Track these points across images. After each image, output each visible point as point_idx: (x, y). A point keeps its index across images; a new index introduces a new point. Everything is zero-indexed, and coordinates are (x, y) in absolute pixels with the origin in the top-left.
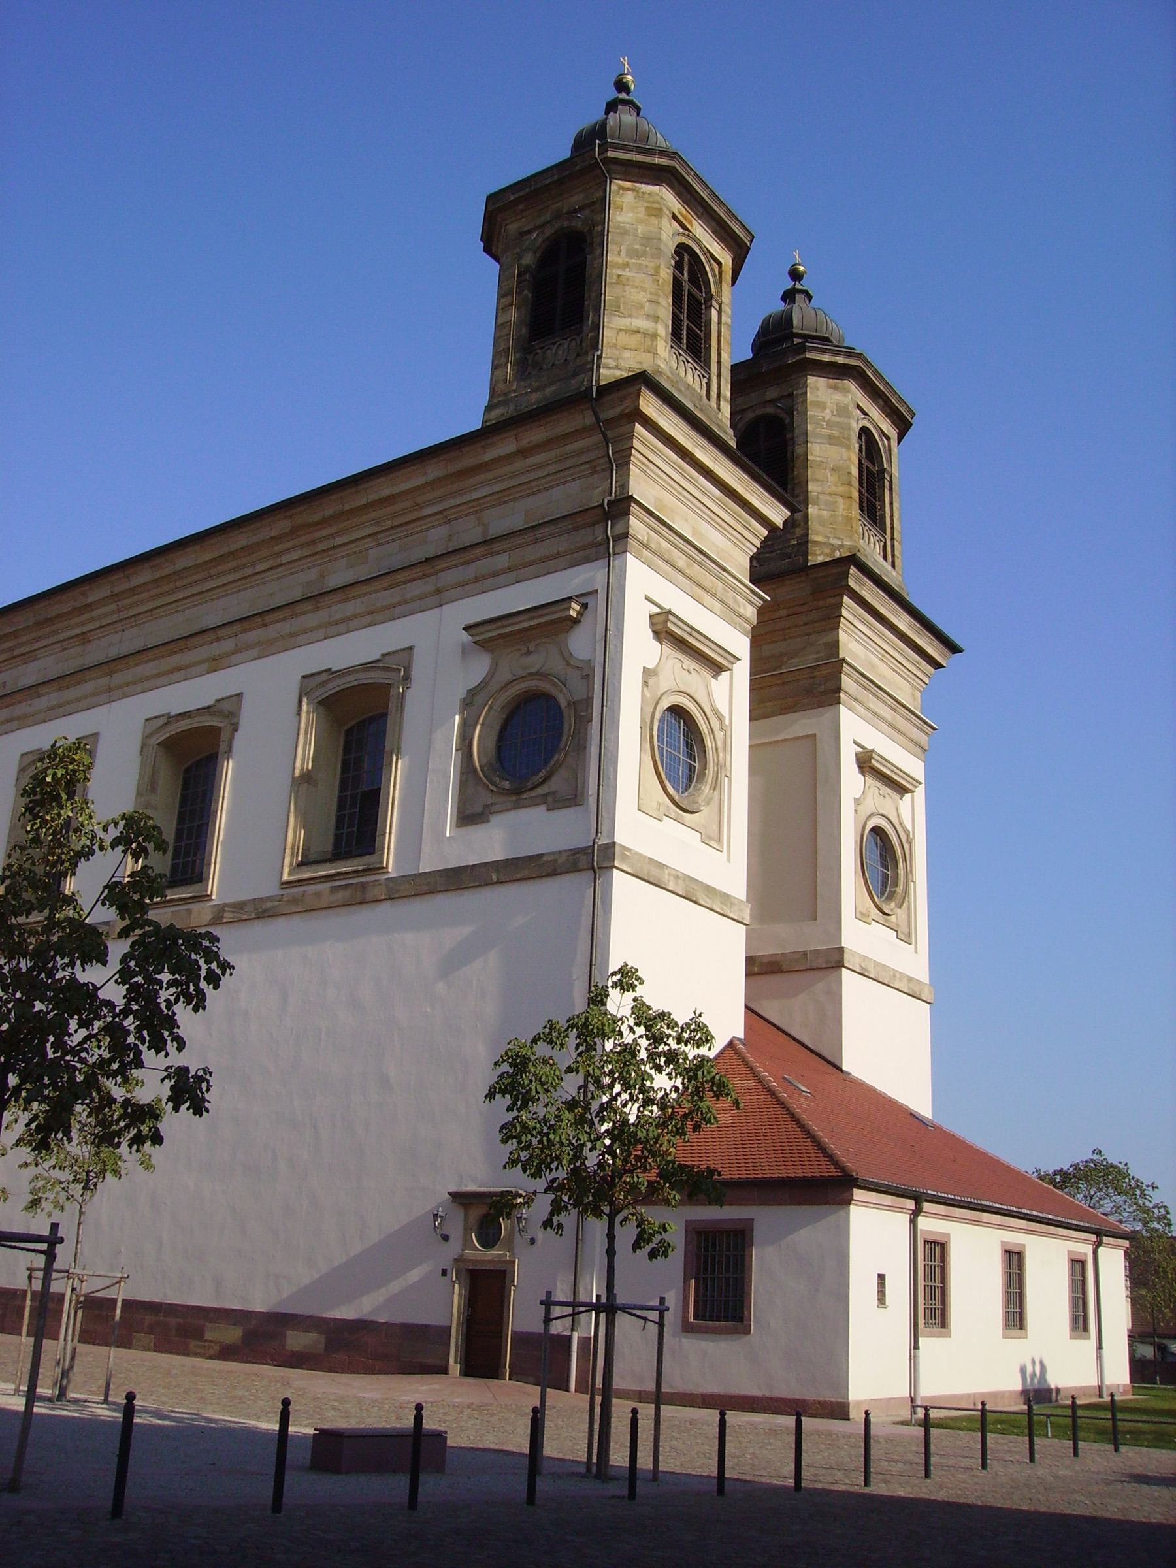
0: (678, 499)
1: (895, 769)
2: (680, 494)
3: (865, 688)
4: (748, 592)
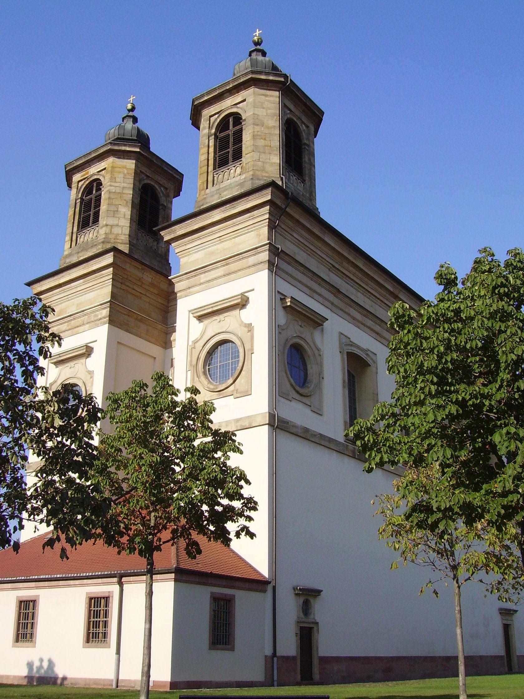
0: (69, 300)
1: (213, 305)
2: (68, 298)
3: (195, 276)
4: (100, 306)
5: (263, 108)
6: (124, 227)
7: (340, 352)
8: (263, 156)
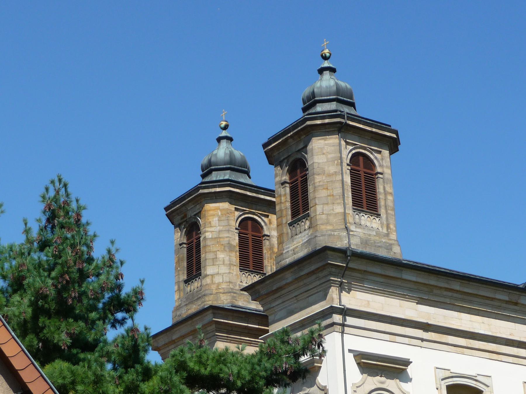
5: (324, 154)
6: (225, 275)
7: (437, 389)
8: (326, 207)
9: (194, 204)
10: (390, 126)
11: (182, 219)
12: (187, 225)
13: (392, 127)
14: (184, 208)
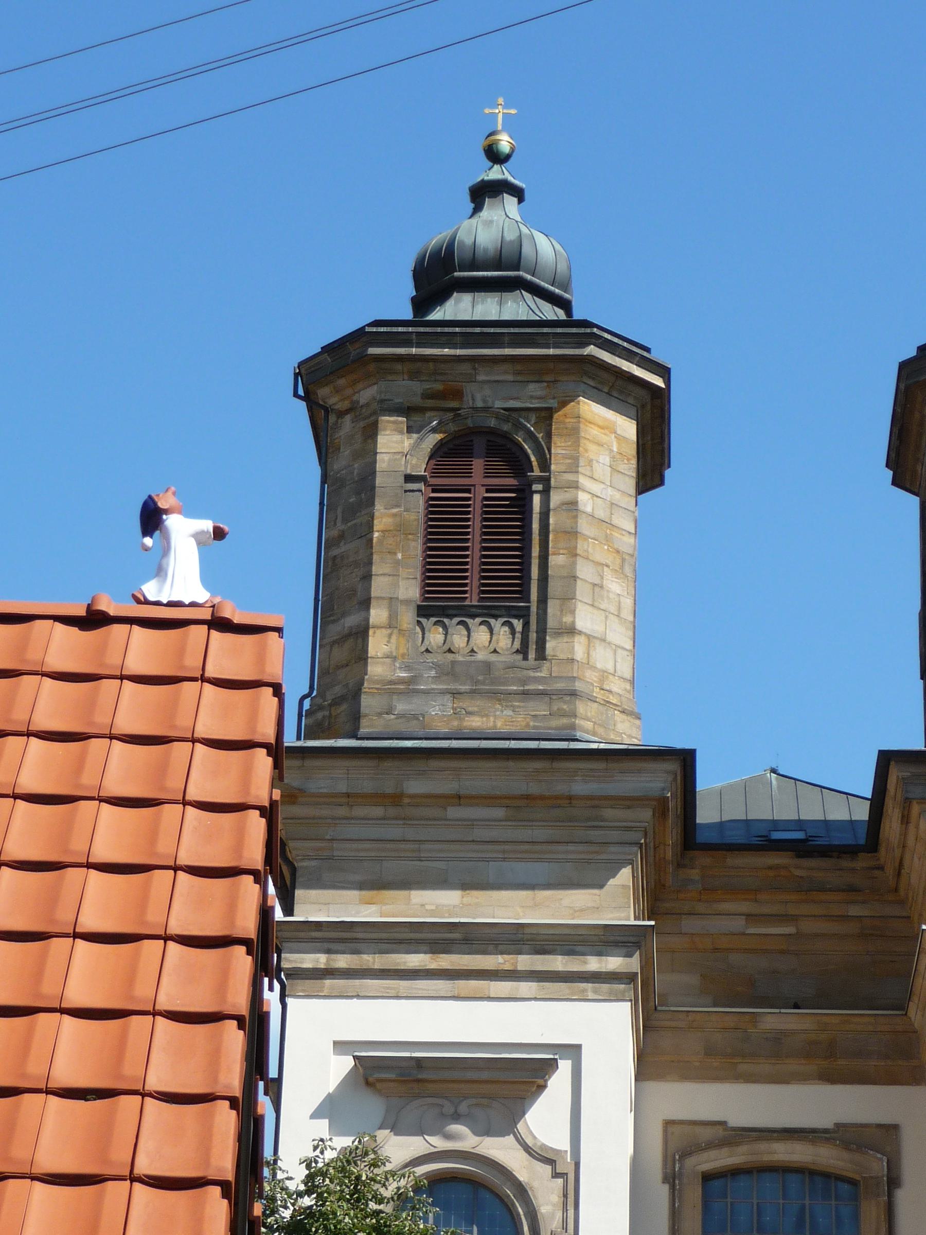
6: (620, 651)
9: (519, 373)
10: (648, 350)
11: (427, 396)
12: (452, 427)
13: (655, 355)
14: (465, 368)
